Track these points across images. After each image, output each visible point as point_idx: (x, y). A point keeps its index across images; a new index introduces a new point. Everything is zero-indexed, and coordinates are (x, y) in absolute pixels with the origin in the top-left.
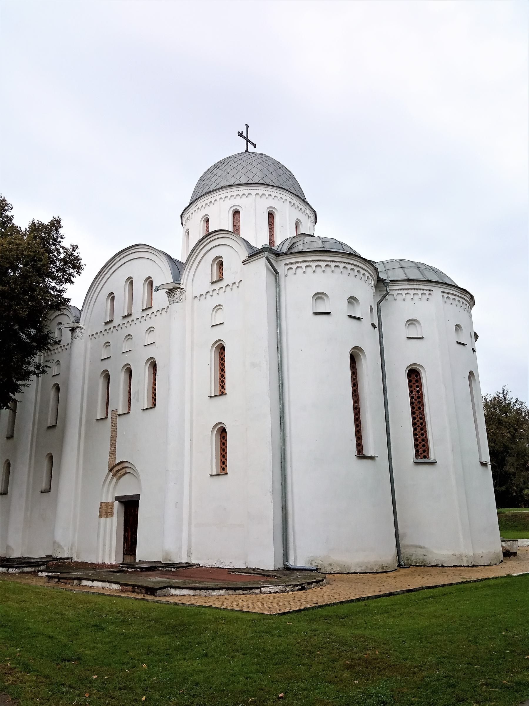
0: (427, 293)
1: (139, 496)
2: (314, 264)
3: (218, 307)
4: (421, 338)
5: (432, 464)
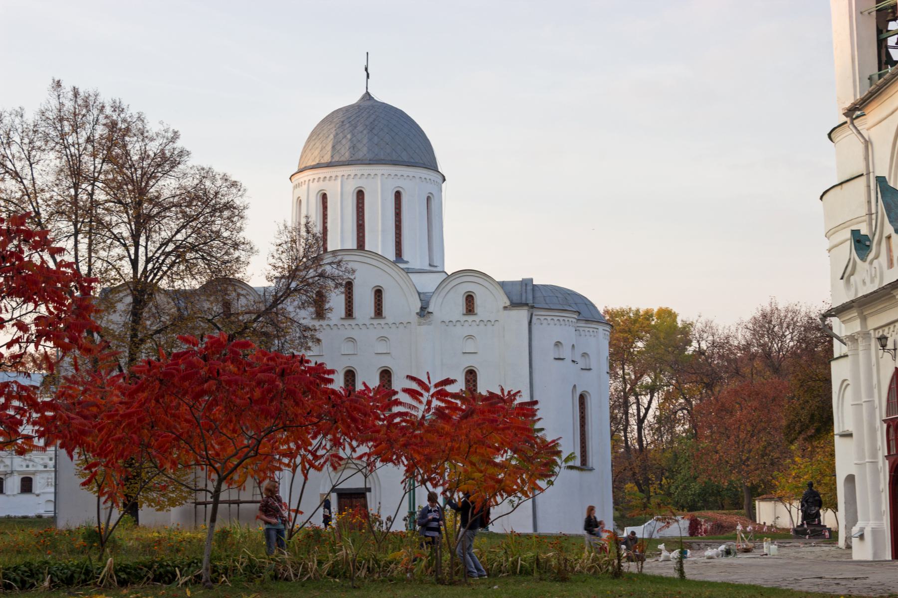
0: (595, 330)
1: (369, 490)
2: (556, 318)
3: (470, 337)
4: (590, 369)
5: (591, 470)
